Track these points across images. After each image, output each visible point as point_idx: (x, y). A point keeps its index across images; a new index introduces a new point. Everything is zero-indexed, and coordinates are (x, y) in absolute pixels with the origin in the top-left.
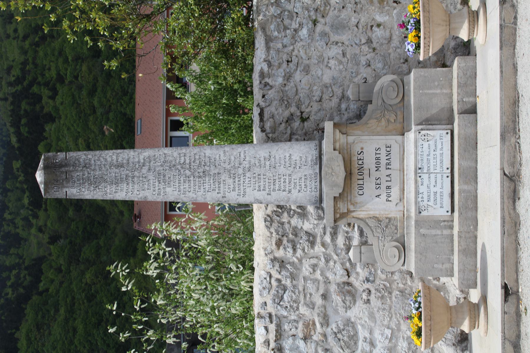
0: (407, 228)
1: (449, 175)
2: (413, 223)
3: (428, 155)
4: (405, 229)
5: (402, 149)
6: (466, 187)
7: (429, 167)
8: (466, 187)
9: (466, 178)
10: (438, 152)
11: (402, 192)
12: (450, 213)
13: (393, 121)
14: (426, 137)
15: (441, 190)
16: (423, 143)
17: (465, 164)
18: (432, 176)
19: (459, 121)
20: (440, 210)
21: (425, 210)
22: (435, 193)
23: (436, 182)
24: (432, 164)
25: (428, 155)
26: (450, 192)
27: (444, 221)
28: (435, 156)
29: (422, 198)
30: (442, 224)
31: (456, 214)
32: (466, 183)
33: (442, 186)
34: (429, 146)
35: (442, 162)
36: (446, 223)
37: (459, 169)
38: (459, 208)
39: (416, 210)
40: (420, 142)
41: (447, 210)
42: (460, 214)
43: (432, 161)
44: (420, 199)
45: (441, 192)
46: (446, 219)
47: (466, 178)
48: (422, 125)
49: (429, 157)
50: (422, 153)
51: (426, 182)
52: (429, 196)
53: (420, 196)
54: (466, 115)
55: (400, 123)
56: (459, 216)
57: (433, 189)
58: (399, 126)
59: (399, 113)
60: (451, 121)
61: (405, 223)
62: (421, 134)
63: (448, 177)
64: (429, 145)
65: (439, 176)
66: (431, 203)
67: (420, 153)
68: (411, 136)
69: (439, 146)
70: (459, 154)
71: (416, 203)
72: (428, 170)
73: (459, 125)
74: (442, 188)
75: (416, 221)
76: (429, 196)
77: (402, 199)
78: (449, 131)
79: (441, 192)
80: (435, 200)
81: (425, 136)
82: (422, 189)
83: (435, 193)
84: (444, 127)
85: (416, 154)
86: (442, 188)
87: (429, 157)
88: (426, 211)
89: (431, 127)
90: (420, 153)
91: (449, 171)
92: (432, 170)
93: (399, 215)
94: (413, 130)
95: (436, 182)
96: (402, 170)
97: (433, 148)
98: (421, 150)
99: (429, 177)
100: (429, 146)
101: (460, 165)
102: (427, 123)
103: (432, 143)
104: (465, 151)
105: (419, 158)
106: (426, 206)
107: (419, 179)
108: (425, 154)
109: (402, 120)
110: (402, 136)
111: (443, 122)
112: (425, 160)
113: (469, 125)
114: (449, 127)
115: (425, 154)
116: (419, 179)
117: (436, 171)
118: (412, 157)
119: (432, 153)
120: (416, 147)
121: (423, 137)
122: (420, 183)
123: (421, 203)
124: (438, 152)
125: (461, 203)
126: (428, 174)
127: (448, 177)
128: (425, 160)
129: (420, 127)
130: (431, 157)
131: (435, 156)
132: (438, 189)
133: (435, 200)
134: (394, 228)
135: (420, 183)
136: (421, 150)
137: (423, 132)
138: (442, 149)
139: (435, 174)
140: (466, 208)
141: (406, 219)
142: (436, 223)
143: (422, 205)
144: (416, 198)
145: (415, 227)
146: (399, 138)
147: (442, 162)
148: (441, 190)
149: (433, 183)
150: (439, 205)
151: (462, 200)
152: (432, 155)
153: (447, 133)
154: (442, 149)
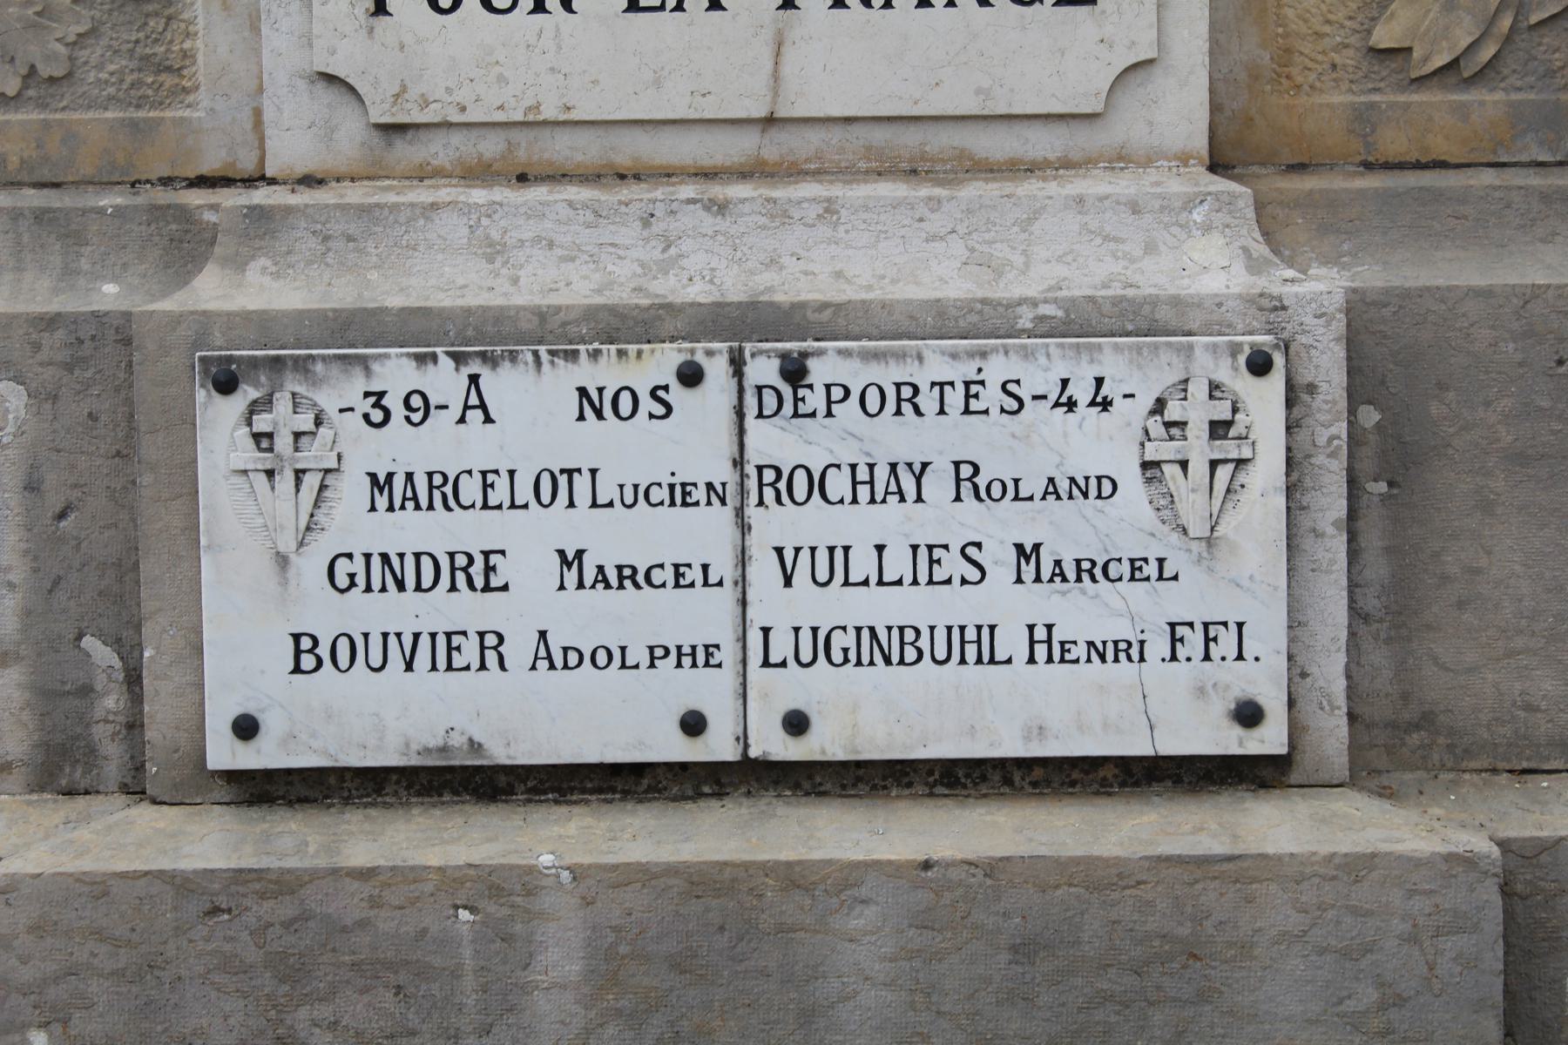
0: (41, 217)
1: (718, 746)
2: (109, 295)
3: (968, 480)
4: (32, 198)
5: (1042, 143)
6: (560, 957)
7: (817, 485)
8: (560, 957)
9: (677, 965)
10: (1008, 605)
11: (490, 146)
12: (224, 753)
13: (1383, 37)
14: (1199, 448)
15: (519, 649)
16: (1130, 413)
17: (864, 946)
18: (703, 534)
19: (1416, 863)
20: (259, 644)
21: (263, 440)
22: (480, 572)
23: (628, 576)
24: (859, 526)
25: (968, 480)
26: (500, 753)
27: (133, 679)
28: (953, 565)
29: (421, 408)
30: (101, 653)
31: (210, 842)
32: (608, 967)
33: (574, 658)
34: (1080, 488)
35: (884, 647)
36: (112, 702)
37: (793, 877)
38: (281, 884)
39: (263, 324)
40: (1135, 375)
41: (272, 724)
42: (213, 897)
43: (895, 524)
44: (397, 374)
45: (492, 645)
46: (161, 712)
47: (677, 965)
48: (1355, 397)
49: (938, 486)
50: (991, 396)
51: (628, 451)
52: (443, 491)
53: (445, 382)
54: (1494, 958)
55: (1363, 119)
56: (182, 884)
57: (529, 541)
58: (1330, 103)
59: (1488, 101)
60: (1397, 743)
61: (111, 200)
62: (1243, 384)
63: (693, 724)
64: (1103, 487)
65: (703, 616)
66: (356, 525)
67: (997, 370)
68: (1211, 260)
69: (1082, 614)
70: (992, 868)
71: (355, 334)
72: (780, 484)
73: (1357, 867)
74: (545, 654)
75: (118, 333)
76: (443, 491)
77: (407, 152)
78: (1270, 739)
79: (492, 645)
80: (392, 572)
81: (1218, 429)
82: (532, 411)
83: (480, 572)
84: (1331, 672)
85: (985, 324)
86: (545, 654)
87: (938, 486)
88: (247, 455)
89: (1331, 504)
90: (997, 370)
91: (773, 744)
92: (776, 525)
93: (208, 125)
94: (1279, 280)
95: (628, 576)
96: (774, 147)
97: (1067, 532)
98: (1038, 378)
99: (681, 495)
100: (1080, 488)
101: (847, 880)
102: (1366, 465)
103: (1128, 521)
104: (1024, 950)
105: (936, 363)
106: (316, 455)
107: (662, 363)
108: (994, 445)
109: (1393, 143)
110: (1201, 143)
111: (1378, 656)
112: (897, 438)
113: (1369, 995)
114: (1332, 736)
115: (994, 445)
116: (662, 363)
117: (764, 571)
118: (945, 278)
119: (999, 527)
120: (1077, 324)
121: (1197, 411)
122: (606, 374)
123: (352, 389)
124: (1008, 605)
125: (350, 903)
126: (723, 473)
127: (693, 724)
128: (897, 438)
129: (1327, 366)
130: (942, 517)
131: (953, 565)
132: (532, 602)
133: (392, 572)
134: (48, 53)
135: (606, 374)
136: (1038, 378)
137: (1264, 402)
138: (1047, 646)
139: (724, 567)
140: (292, 972)
141: (157, 212)
142: (112, 568)
143: (328, 400)
144: (421, 332)
145: (51, 322)
146: (1180, 110)
147: (884, 647)
148: (519, 649)
149: (613, 538)
150: (328, 616)
151: (386, 922)
152: (971, 519)
153: (1249, 715)
154: (1047, 646)
